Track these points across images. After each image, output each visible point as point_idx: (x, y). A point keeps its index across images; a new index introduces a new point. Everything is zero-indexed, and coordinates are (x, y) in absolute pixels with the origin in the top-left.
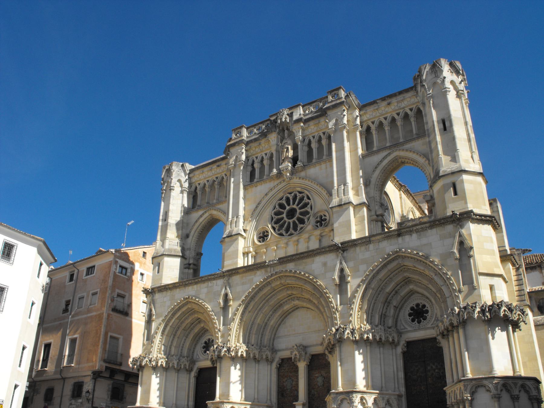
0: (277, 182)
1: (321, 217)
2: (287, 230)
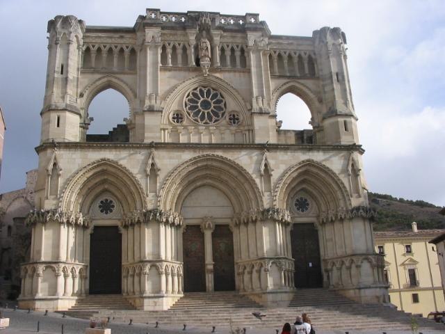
2: (202, 118)
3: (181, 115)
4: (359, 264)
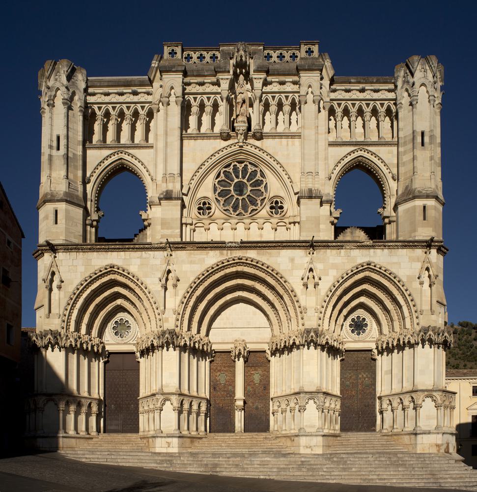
0: (225, 144)
1: (277, 202)
2: (235, 208)
3: (209, 204)
4: (420, 402)
